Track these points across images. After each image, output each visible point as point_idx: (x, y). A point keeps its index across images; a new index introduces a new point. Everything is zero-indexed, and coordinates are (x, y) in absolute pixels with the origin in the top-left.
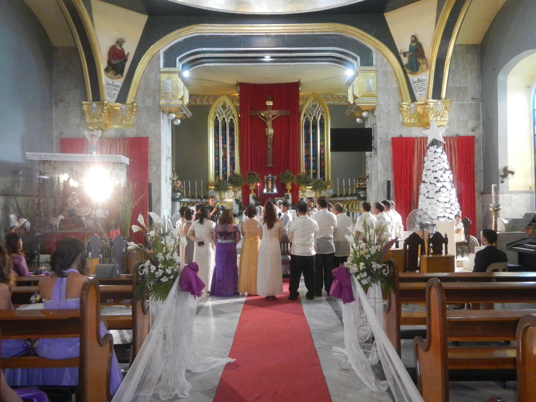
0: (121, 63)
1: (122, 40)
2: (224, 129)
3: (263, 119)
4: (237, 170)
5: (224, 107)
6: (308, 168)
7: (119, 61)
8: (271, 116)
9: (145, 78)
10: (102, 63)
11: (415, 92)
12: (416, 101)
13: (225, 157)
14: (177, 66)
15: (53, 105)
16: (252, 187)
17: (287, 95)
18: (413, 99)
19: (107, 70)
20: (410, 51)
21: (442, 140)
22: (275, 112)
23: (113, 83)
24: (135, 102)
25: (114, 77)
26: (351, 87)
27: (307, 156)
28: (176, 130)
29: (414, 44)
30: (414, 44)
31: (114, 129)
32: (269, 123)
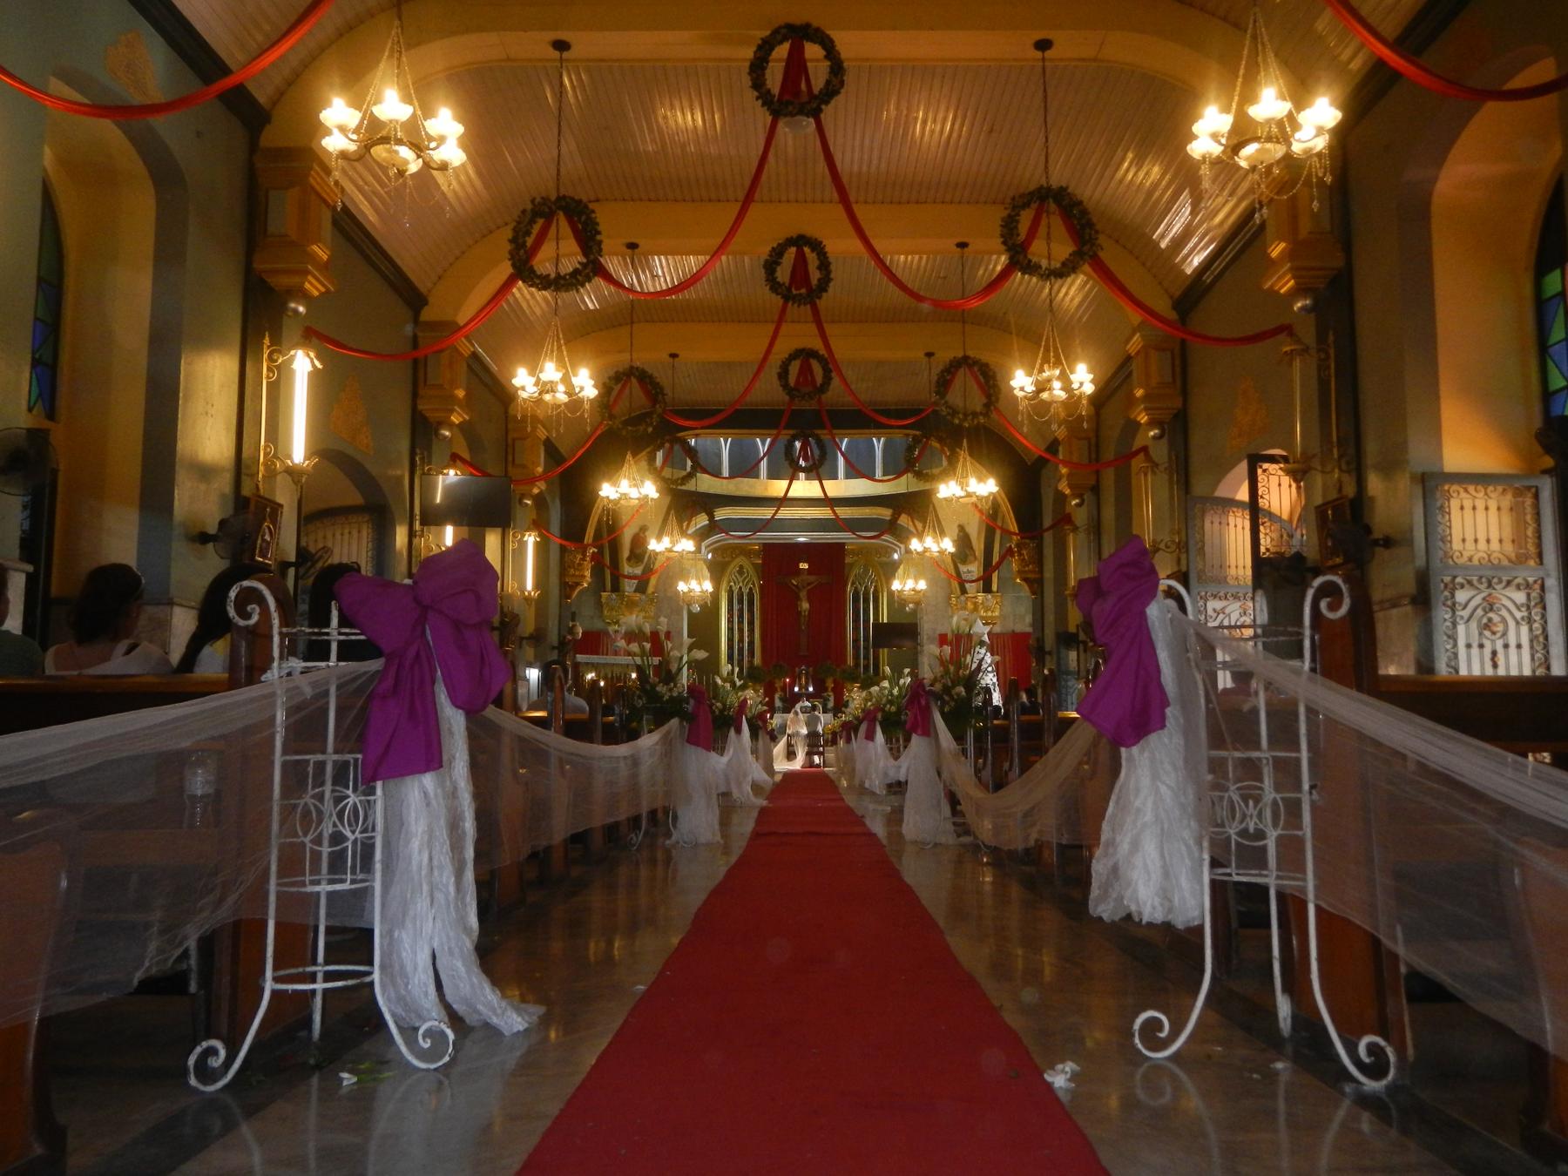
2: (741, 602)
4: (757, 661)
5: (741, 572)
6: (856, 657)
10: (626, 553)
13: (741, 640)
16: (778, 684)
18: (964, 591)
19: (629, 559)
21: (986, 638)
22: (812, 578)
27: (856, 641)
28: (690, 613)
31: (632, 619)
32: (803, 594)
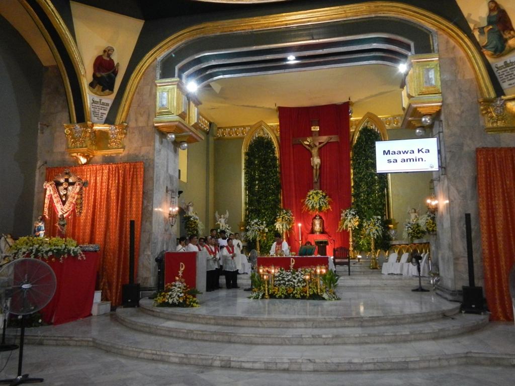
0: (109, 76)
1: (109, 48)
3: (307, 147)
7: (106, 74)
8: (317, 144)
9: (138, 93)
11: (501, 82)
12: (504, 95)
14: (176, 75)
15: (39, 131)
17: (335, 116)
19: (92, 85)
20: (489, 23)
22: (324, 139)
23: (101, 100)
24: (125, 123)
25: (102, 93)
26: (405, 88)
29: (495, 13)
30: (495, 13)
32: (315, 151)
